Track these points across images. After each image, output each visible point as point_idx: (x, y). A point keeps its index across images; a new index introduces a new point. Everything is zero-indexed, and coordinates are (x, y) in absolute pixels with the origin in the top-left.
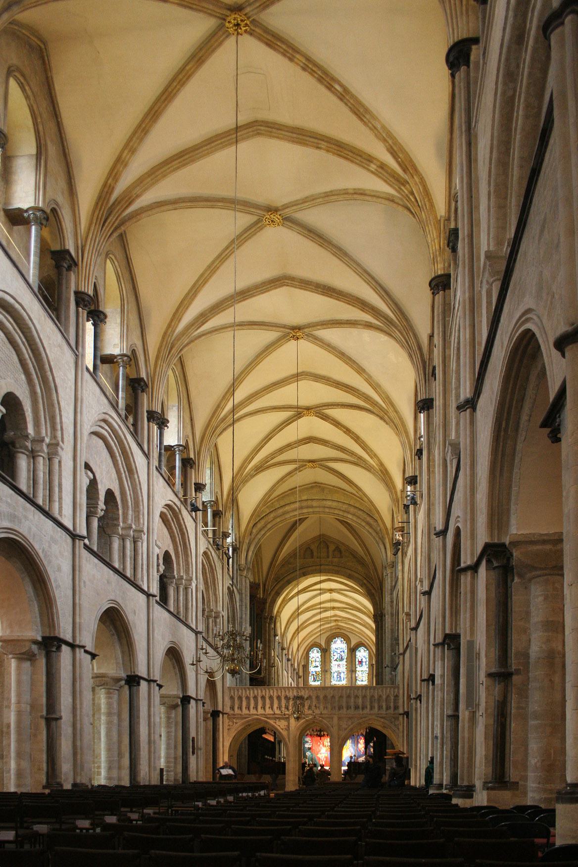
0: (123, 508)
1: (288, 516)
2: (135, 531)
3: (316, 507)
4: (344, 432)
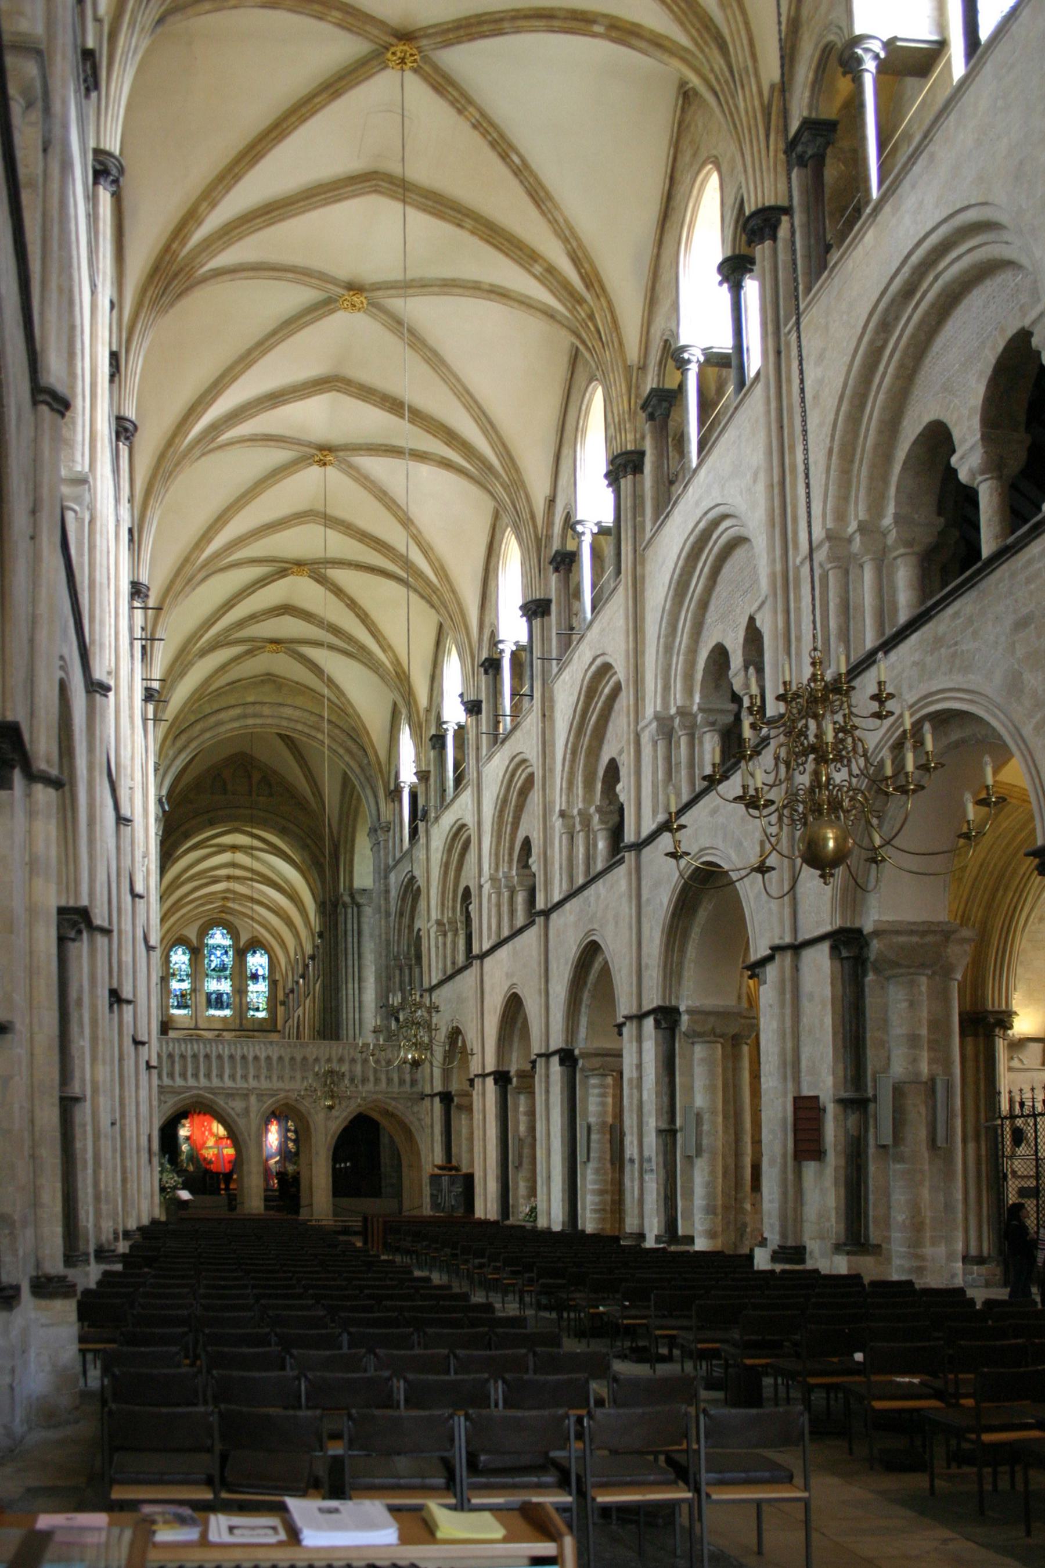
1: (222, 729)
3: (268, 716)
4: (347, 605)
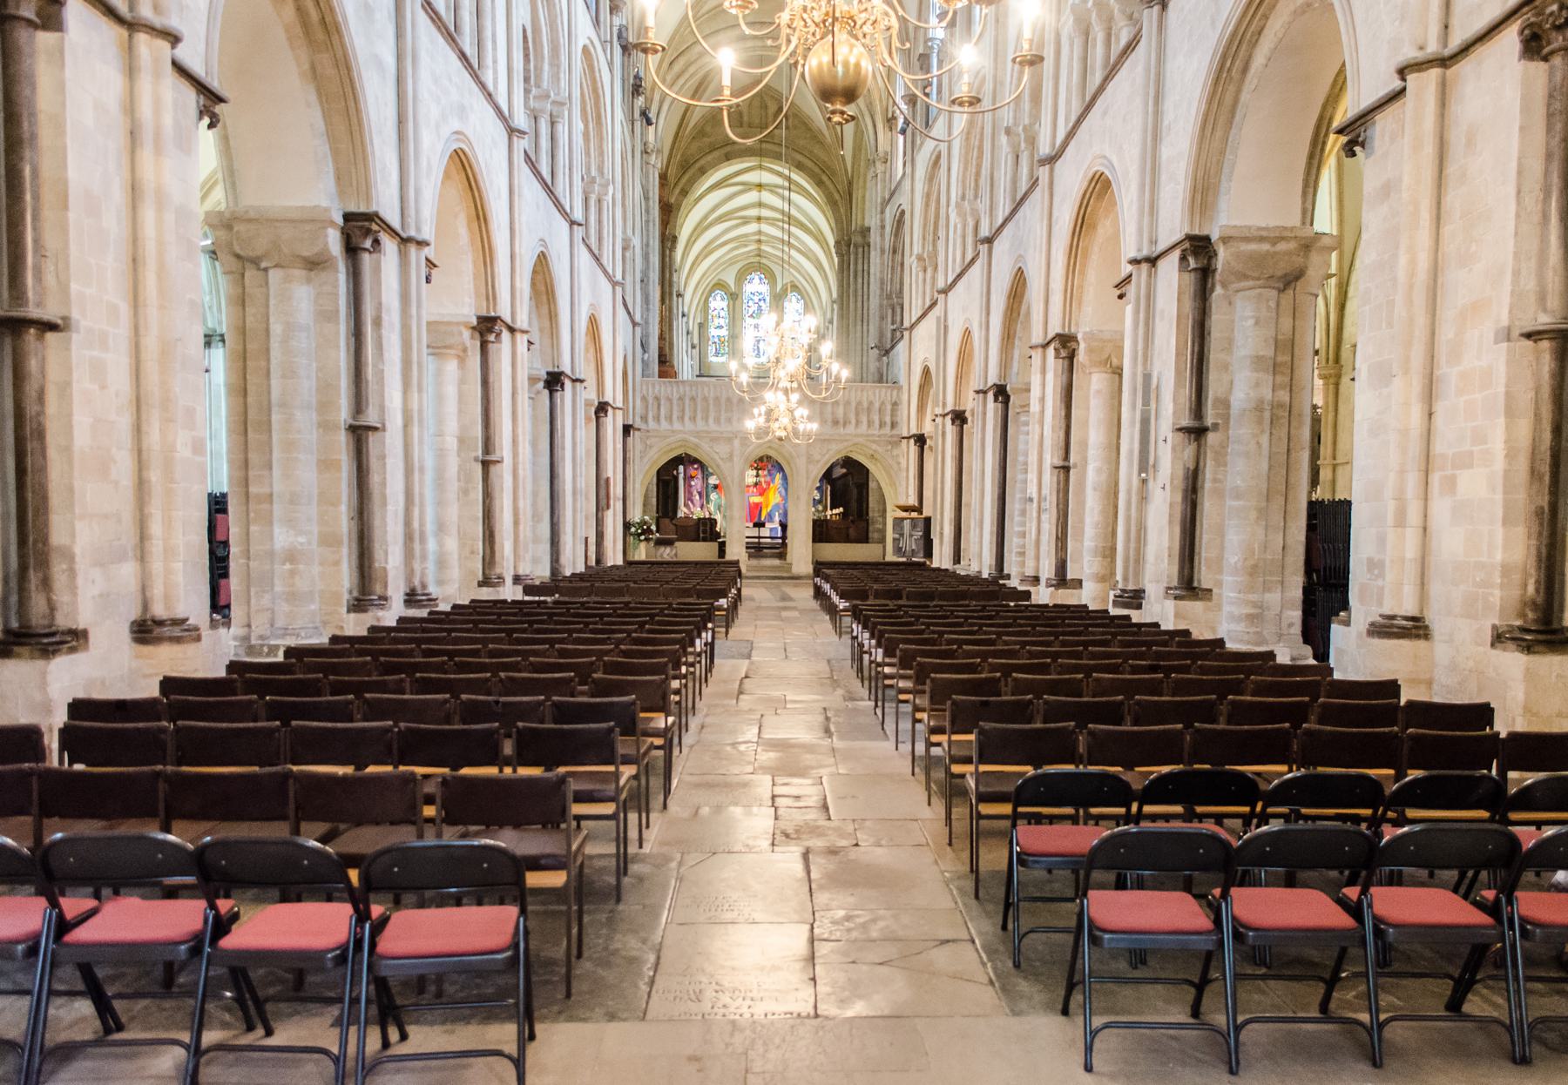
0: (536, 59)
2: (554, 102)
